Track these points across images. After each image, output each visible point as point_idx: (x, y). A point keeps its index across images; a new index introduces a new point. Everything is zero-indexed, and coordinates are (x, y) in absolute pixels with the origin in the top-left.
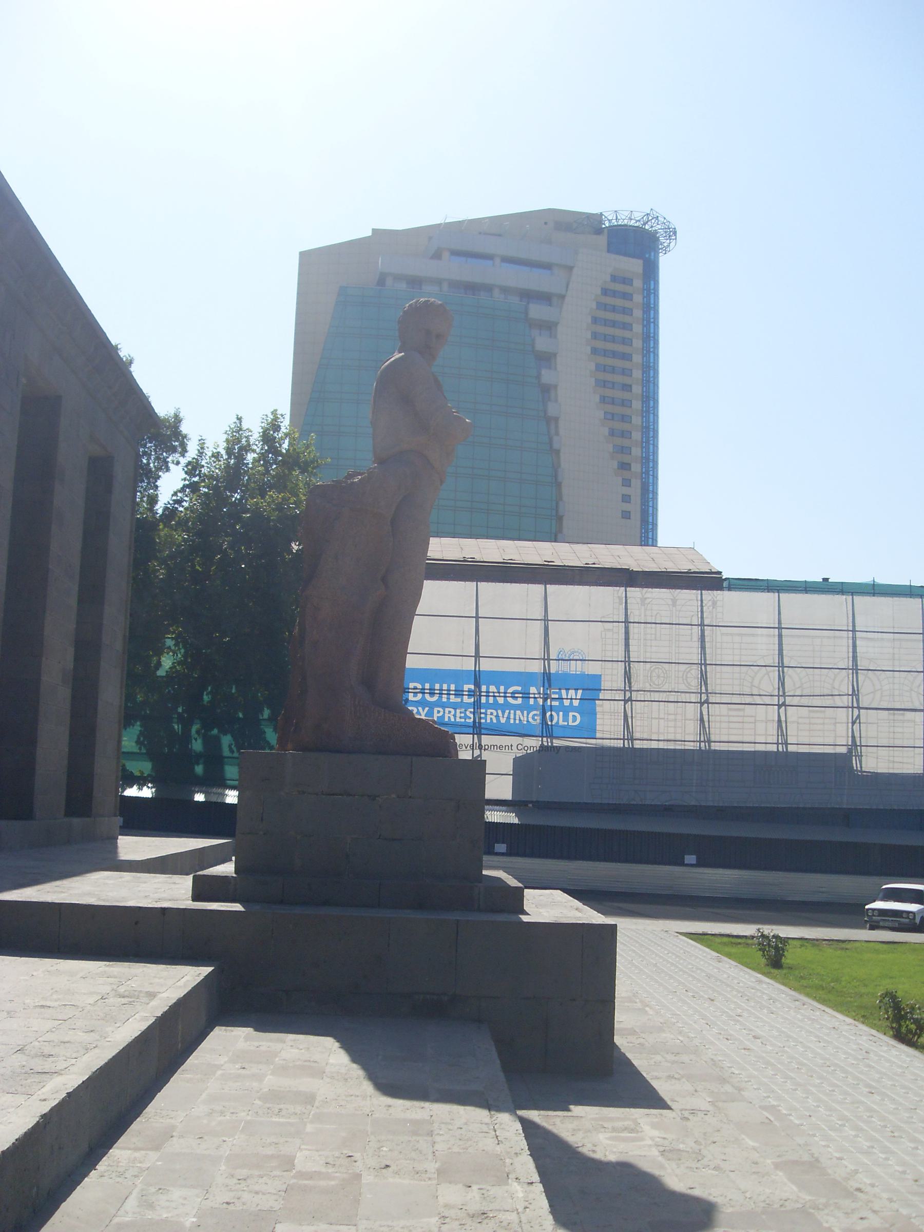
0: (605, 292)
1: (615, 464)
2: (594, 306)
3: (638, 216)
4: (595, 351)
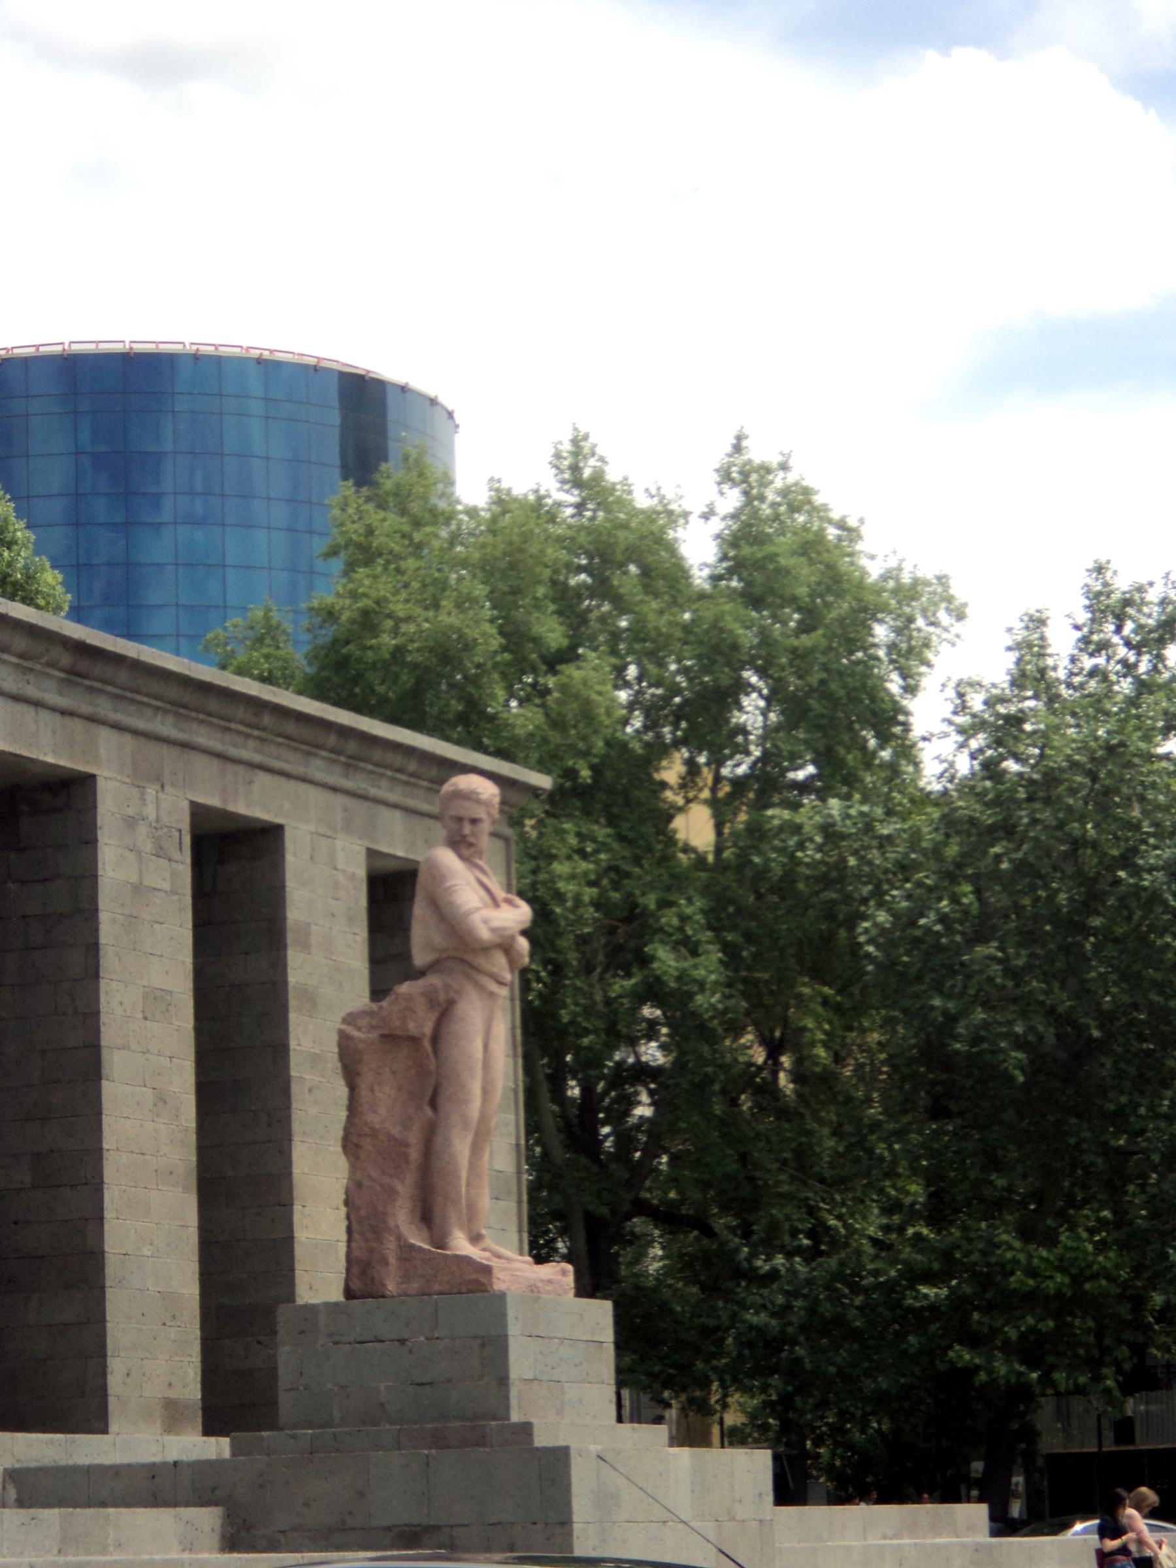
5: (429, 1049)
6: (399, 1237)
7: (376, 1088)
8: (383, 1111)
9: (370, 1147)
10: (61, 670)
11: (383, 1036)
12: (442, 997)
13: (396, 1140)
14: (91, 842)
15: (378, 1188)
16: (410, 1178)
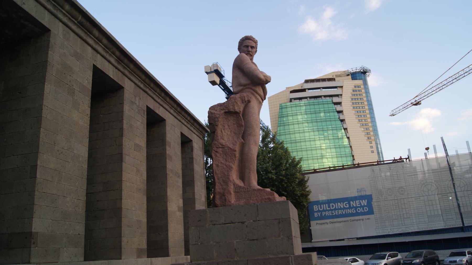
0: (354, 91)
1: (366, 138)
2: (351, 95)
3: (358, 68)
4: (354, 107)
6: (234, 184)
7: (223, 131)
8: (226, 139)
9: (221, 152)
10: (115, 56)
11: (225, 112)
13: (231, 149)
14: (122, 104)
15: (225, 167)
16: (236, 163)
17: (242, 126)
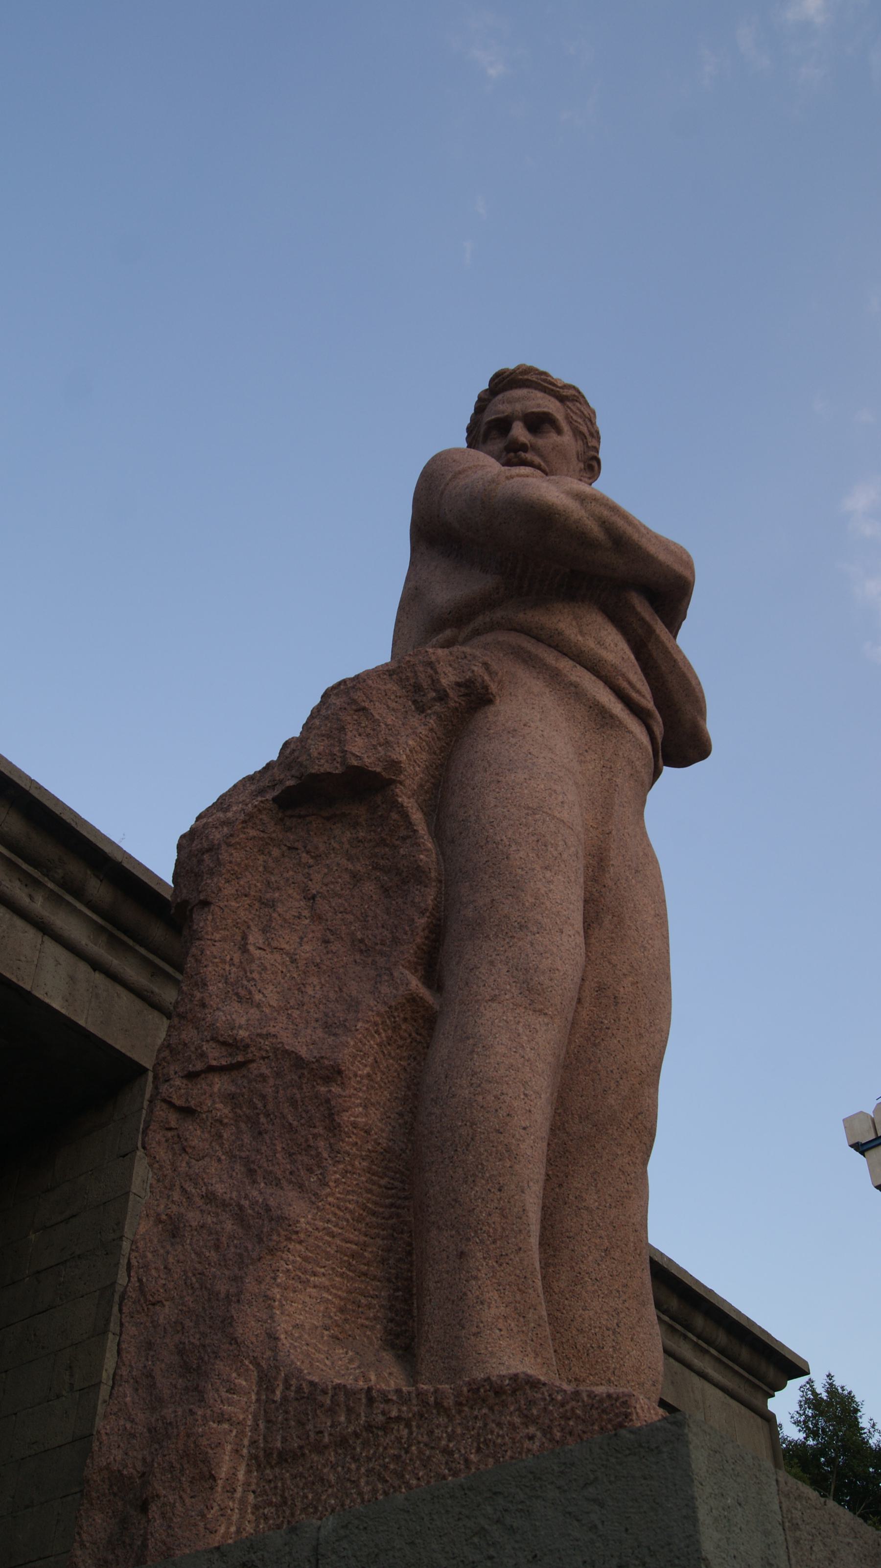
5: (417, 816)
7: (255, 938)
8: (271, 996)
9: (223, 1110)
10: (89, 905)
12: (448, 678)
13: (299, 1062)
15: (229, 1226)
17: (418, 875)
